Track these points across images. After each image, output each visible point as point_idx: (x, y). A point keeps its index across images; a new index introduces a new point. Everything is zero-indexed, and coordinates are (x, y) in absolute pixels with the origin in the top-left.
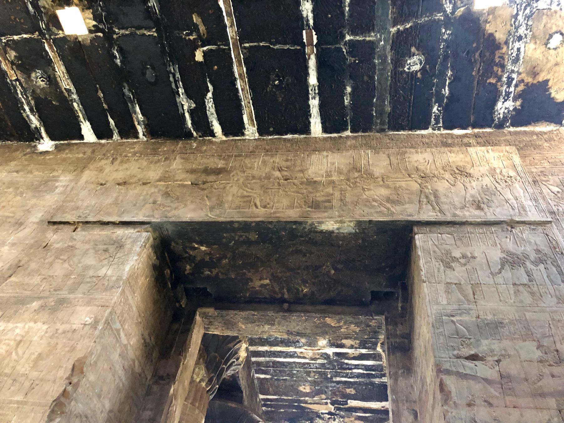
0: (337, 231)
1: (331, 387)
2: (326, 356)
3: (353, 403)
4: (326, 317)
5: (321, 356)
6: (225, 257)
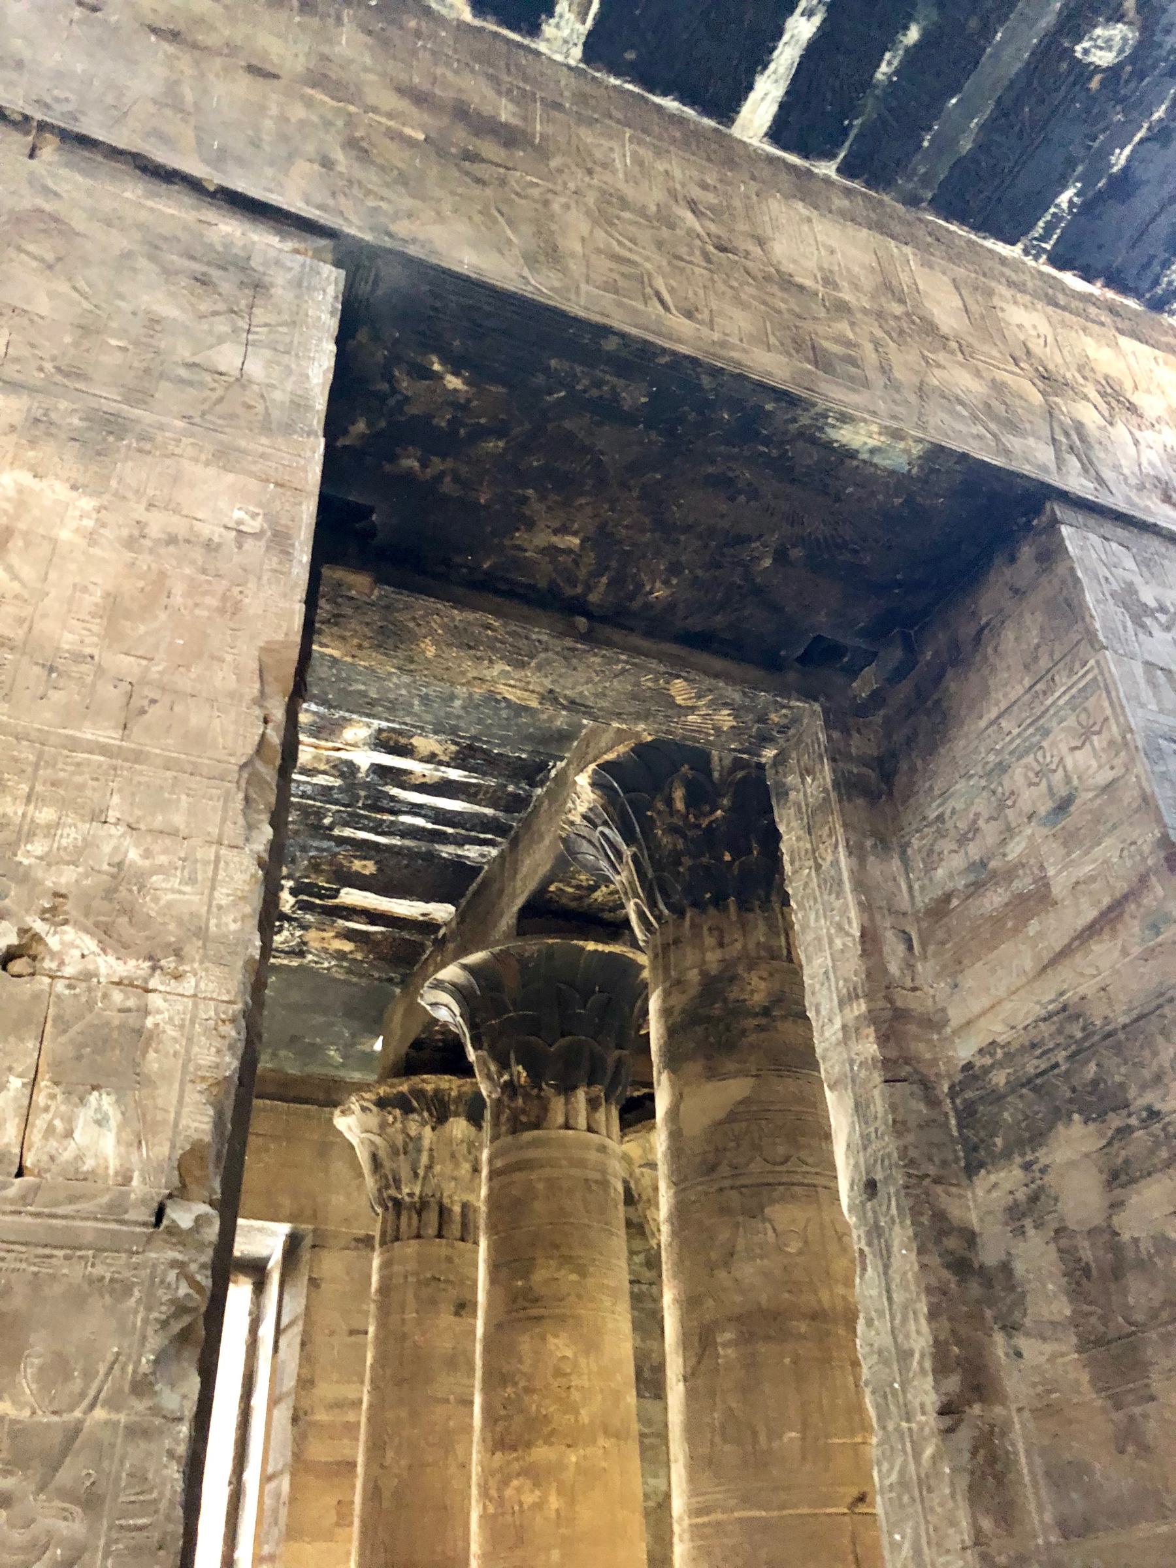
0: (865, 456)
1: (317, 849)
2: (347, 770)
3: (351, 896)
4: (678, 677)
5: (334, 767)
6: (500, 431)
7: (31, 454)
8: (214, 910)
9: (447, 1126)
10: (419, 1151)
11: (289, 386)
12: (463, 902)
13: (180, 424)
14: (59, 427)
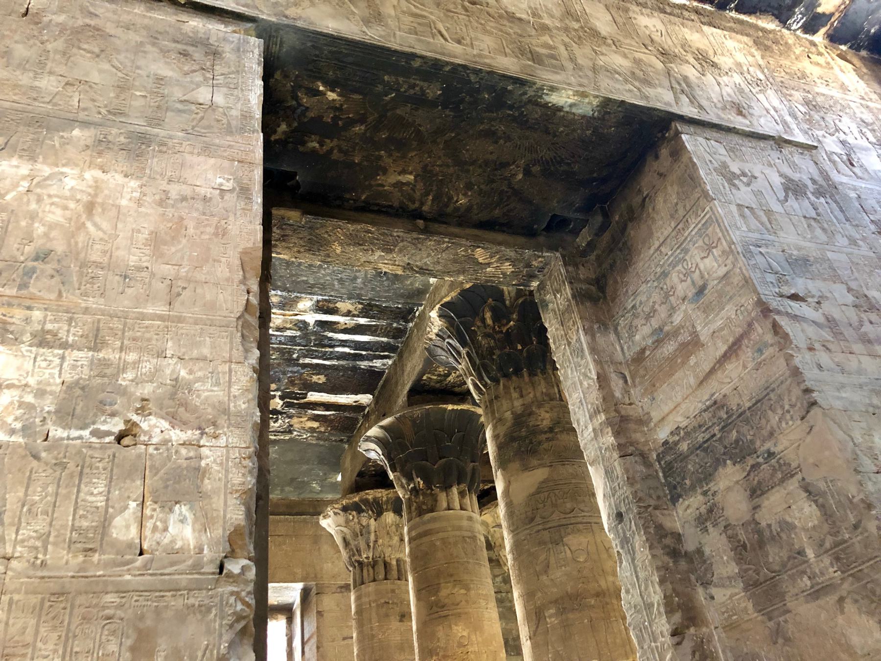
0: (567, 109)
1: (291, 372)
2: (303, 326)
3: (314, 397)
4: (479, 247)
5: (295, 325)
6: (362, 120)
7: (99, 160)
8: (232, 398)
9: (383, 517)
10: (369, 533)
11: (239, 106)
12: (376, 392)
13: (180, 134)
14: (114, 144)
